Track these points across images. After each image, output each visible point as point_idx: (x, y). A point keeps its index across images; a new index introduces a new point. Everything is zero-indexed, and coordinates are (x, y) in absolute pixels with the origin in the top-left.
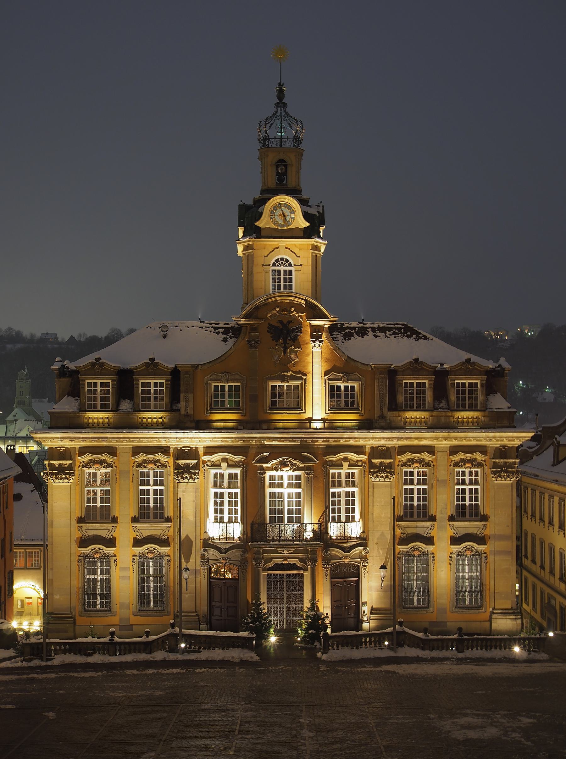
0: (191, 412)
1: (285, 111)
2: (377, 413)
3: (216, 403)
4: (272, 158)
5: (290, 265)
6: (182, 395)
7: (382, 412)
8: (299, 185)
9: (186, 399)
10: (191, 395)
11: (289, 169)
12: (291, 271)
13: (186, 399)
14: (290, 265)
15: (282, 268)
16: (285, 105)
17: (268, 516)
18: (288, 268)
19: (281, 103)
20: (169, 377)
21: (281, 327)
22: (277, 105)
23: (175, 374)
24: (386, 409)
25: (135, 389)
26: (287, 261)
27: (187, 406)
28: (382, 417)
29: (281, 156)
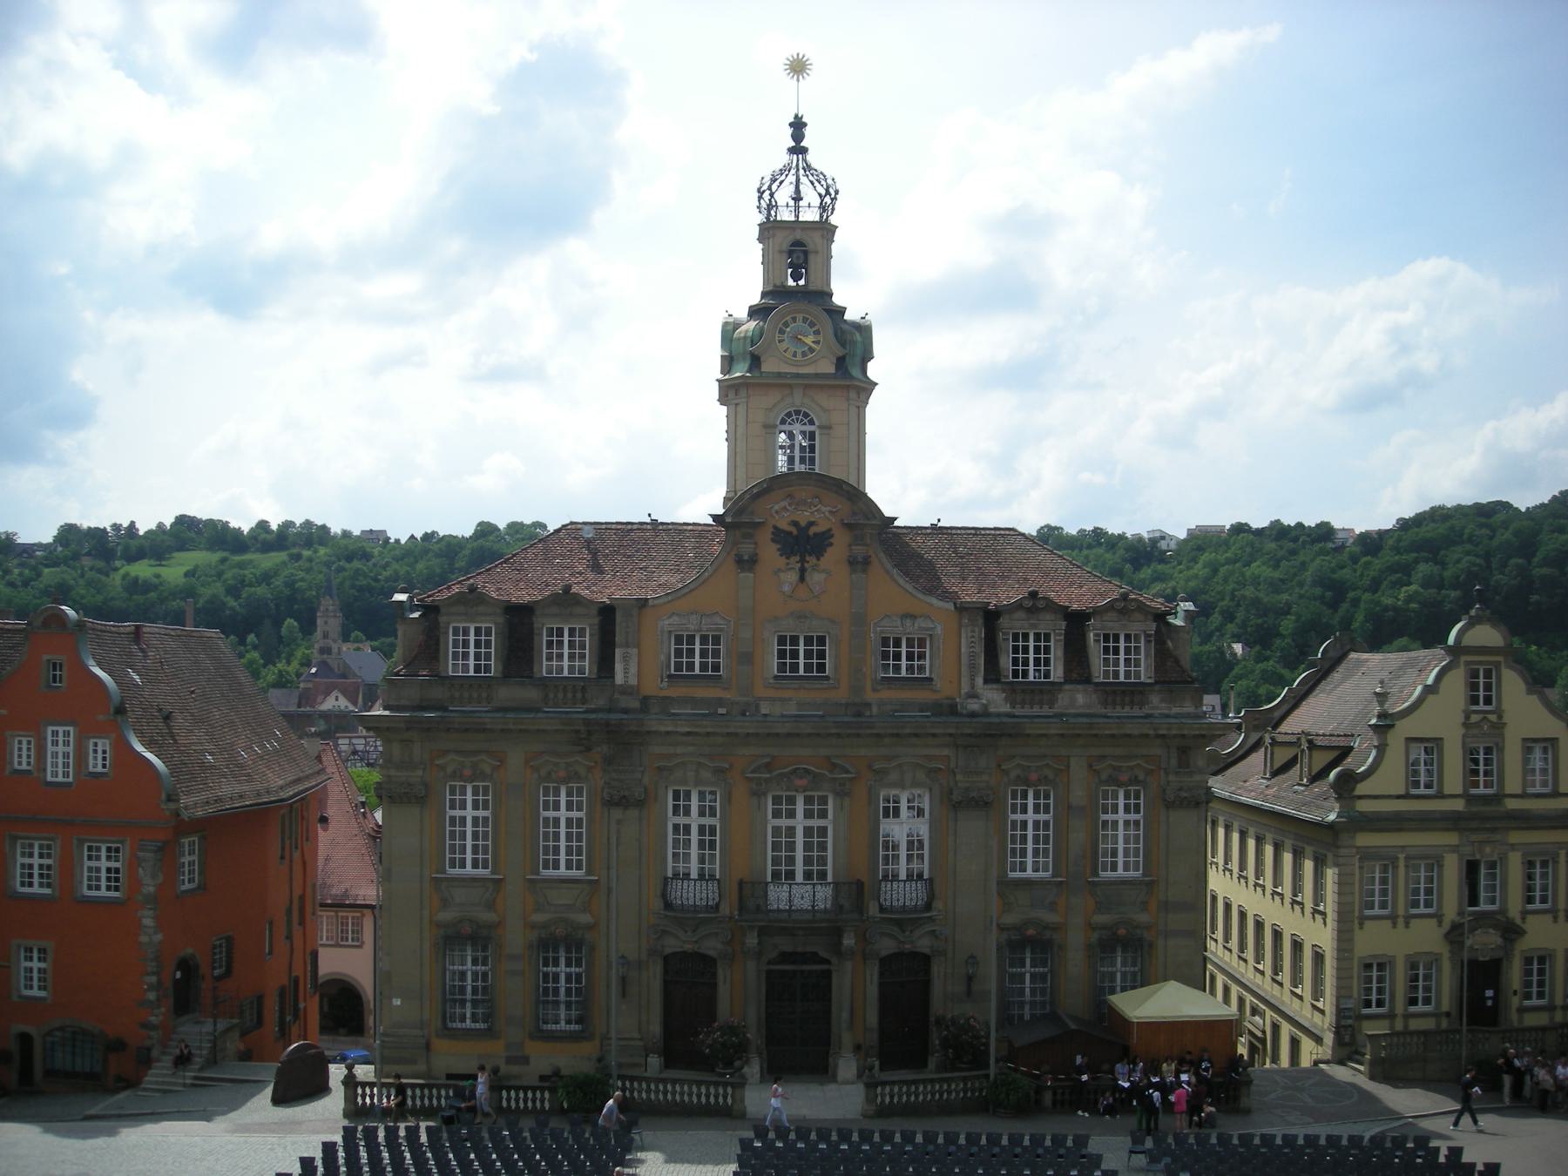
0: (633, 681)
1: (805, 160)
2: (965, 689)
3: (678, 666)
4: (783, 240)
5: (812, 422)
6: (618, 652)
7: (973, 686)
8: (829, 284)
9: (625, 659)
10: (634, 651)
11: (812, 258)
12: (812, 436)
13: (625, 659)
14: (812, 422)
15: (797, 429)
16: (804, 151)
17: (770, 868)
18: (809, 428)
19: (798, 150)
20: (596, 621)
21: (795, 532)
22: (792, 151)
23: (607, 613)
24: (980, 680)
25: (536, 638)
26: (806, 415)
27: (626, 672)
28: (973, 695)
29: (798, 235)
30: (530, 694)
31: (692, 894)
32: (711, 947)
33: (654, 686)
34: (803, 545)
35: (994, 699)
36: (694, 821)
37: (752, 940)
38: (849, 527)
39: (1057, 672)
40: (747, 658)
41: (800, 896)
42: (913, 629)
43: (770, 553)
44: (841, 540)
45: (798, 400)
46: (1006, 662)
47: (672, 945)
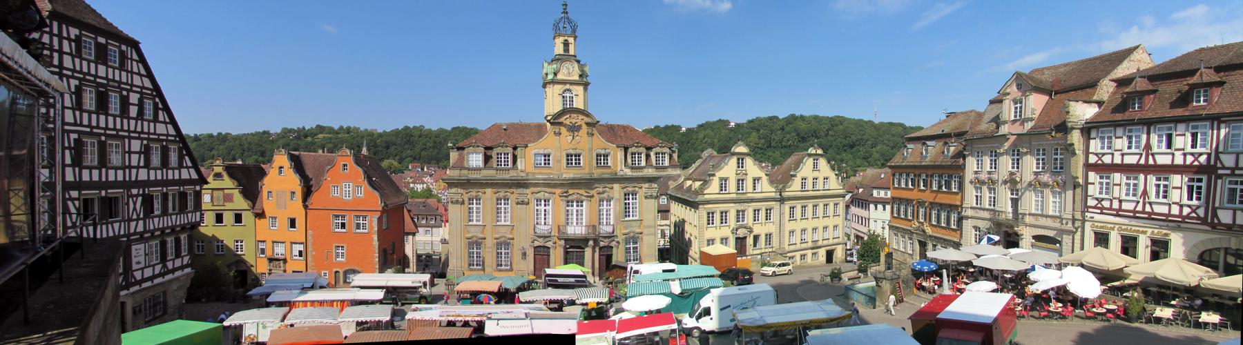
30: (492, 172)
31: (542, 229)
32: (549, 244)
33: (530, 169)
34: (574, 129)
35: (628, 172)
36: (542, 208)
37: (562, 242)
38: (587, 124)
39: (643, 163)
40: (559, 161)
41: (576, 230)
42: (603, 152)
43: (563, 130)
44: (584, 127)
45: (568, 86)
46: (629, 160)
47: (537, 243)
